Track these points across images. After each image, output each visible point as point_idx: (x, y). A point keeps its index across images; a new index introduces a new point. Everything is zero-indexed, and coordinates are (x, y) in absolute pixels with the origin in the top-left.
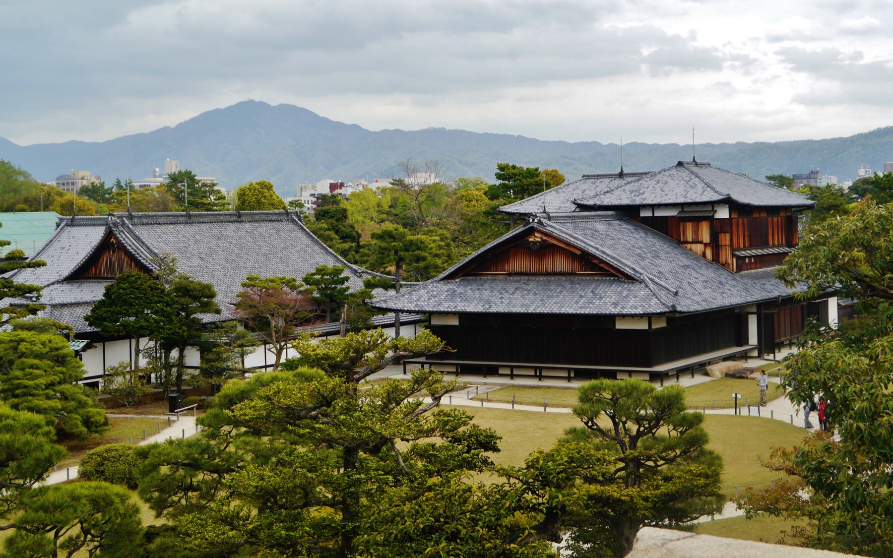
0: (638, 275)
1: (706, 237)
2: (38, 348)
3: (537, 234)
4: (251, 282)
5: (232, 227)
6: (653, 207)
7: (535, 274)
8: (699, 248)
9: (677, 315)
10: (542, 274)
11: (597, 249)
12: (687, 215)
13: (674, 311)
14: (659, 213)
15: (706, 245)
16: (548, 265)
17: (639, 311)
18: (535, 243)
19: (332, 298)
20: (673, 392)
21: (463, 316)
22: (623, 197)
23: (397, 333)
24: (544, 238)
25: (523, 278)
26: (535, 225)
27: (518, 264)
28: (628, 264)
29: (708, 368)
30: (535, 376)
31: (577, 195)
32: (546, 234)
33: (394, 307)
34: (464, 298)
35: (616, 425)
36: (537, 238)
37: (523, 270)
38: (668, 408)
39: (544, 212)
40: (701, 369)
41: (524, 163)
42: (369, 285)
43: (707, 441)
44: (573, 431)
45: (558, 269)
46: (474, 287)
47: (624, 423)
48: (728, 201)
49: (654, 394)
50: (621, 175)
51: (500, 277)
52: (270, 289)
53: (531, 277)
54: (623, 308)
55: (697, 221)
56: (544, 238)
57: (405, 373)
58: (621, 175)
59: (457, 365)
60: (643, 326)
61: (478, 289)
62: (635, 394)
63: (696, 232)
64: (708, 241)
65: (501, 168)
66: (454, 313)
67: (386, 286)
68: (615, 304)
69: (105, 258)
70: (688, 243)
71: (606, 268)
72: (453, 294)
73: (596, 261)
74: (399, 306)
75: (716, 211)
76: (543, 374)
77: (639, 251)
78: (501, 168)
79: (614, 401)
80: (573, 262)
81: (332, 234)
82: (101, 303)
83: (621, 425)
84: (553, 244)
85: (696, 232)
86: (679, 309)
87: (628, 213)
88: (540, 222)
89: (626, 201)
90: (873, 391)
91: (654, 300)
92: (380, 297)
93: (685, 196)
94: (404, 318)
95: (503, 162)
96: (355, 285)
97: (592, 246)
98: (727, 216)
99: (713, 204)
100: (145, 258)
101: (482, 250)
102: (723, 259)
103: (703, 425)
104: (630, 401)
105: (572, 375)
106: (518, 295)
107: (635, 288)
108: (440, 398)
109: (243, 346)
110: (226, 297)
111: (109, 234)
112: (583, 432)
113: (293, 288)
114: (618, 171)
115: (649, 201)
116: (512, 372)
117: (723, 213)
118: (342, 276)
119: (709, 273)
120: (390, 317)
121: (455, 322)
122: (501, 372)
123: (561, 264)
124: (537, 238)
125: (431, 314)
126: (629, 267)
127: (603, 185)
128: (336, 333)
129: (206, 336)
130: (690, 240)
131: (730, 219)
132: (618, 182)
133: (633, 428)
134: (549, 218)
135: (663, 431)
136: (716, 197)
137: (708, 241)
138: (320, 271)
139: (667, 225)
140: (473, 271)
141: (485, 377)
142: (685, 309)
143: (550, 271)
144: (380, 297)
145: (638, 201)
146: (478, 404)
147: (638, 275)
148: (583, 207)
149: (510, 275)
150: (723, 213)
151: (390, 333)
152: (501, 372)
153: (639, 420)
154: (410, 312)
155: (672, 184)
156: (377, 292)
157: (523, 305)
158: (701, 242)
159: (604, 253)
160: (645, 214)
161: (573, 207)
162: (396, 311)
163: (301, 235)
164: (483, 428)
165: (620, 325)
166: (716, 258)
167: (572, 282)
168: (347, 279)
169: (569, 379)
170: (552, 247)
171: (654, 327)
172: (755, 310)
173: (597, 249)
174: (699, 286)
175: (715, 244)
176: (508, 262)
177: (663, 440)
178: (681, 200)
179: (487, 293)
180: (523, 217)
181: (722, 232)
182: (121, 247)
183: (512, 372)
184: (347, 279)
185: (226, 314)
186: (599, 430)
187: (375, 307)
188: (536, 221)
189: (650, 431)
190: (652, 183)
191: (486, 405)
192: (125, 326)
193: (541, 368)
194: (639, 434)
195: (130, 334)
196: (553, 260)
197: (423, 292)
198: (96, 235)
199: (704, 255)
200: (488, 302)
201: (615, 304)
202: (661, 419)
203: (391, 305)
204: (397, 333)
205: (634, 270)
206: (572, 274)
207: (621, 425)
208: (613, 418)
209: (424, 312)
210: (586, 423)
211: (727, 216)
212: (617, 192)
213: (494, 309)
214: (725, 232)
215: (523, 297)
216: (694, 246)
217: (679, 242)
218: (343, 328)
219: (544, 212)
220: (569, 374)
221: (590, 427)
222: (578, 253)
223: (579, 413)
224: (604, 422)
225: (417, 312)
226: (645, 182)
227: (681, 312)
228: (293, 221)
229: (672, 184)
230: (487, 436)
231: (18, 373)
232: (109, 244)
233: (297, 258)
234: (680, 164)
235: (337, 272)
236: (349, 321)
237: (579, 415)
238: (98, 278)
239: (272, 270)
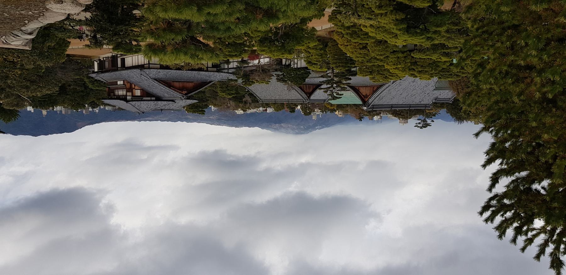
2: (315, 66)
4: (268, 82)
5: (277, 98)
6: (151, 100)
16: (181, 85)
17: (152, 70)
22: (160, 104)
27: (191, 85)
28: (156, 84)
31: (175, 105)
36: (184, 92)
48: (127, 101)
50: (162, 110)
52: (263, 80)
67: (231, 80)
68: (159, 72)
69: (311, 90)
82: (307, 77)
87: (158, 99)
89: (159, 102)
94: (226, 71)
96: (240, 81)
97: (167, 89)
99: (132, 101)
100: (299, 90)
101: (201, 89)
102: (129, 84)
107: (154, 77)
109: (269, 65)
110: (274, 79)
111: (309, 97)
113: (257, 81)
119: (132, 80)
120: (230, 71)
123: (177, 84)
124: (184, 92)
125: (217, 72)
127: (167, 107)
128: (244, 67)
129: (278, 67)
132: (163, 108)
136: (131, 102)
138: (251, 85)
139: (147, 95)
140: (204, 83)
145: (155, 102)
148: (173, 101)
155: (145, 107)
160: (154, 98)
163: (259, 96)
166: (131, 84)
170: (180, 89)
174: (135, 77)
178: (142, 102)
182: (306, 93)
185: (274, 73)
190: (152, 107)
192: (300, 72)
195: (298, 69)
198: (312, 97)
201: (159, 72)
212: (162, 105)
217: (143, 90)
224: (134, 43)
226: (153, 108)
229: (145, 107)
231: (320, 60)
232: (310, 94)
233: (258, 89)
236: (241, 70)
238: (310, 85)
239: (264, 85)
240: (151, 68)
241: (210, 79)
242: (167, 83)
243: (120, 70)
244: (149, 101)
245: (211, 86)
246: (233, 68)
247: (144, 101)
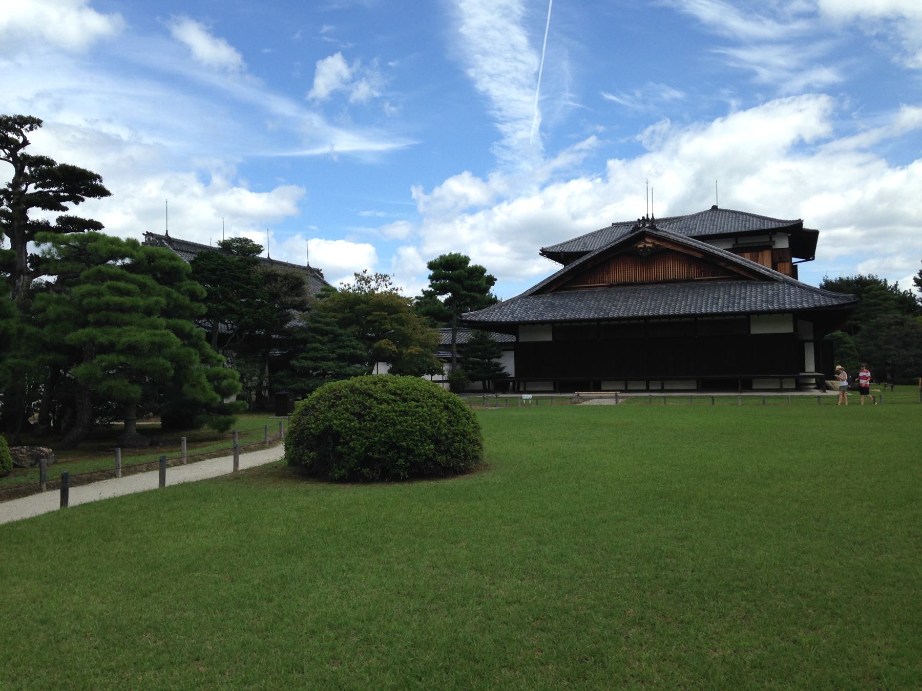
3: (647, 240)
7: (642, 284)
10: (650, 283)
24: (657, 243)
25: (627, 288)
27: (620, 273)
51: (599, 289)
56: (657, 243)
71: (734, 270)
73: (722, 264)
84: (668, 249)
121: (548, 338)
123: (674, 270)
124: (649, 243)
149: (611, 286)
165: (756, 330)
172: (811, 337)
176: (608, 273)
187: (466, 321)
188: (647, 225)
206: (689, 280)
214: (785, 262)
222: (699, 256)
228: (315, 277)
234: (715, 208)
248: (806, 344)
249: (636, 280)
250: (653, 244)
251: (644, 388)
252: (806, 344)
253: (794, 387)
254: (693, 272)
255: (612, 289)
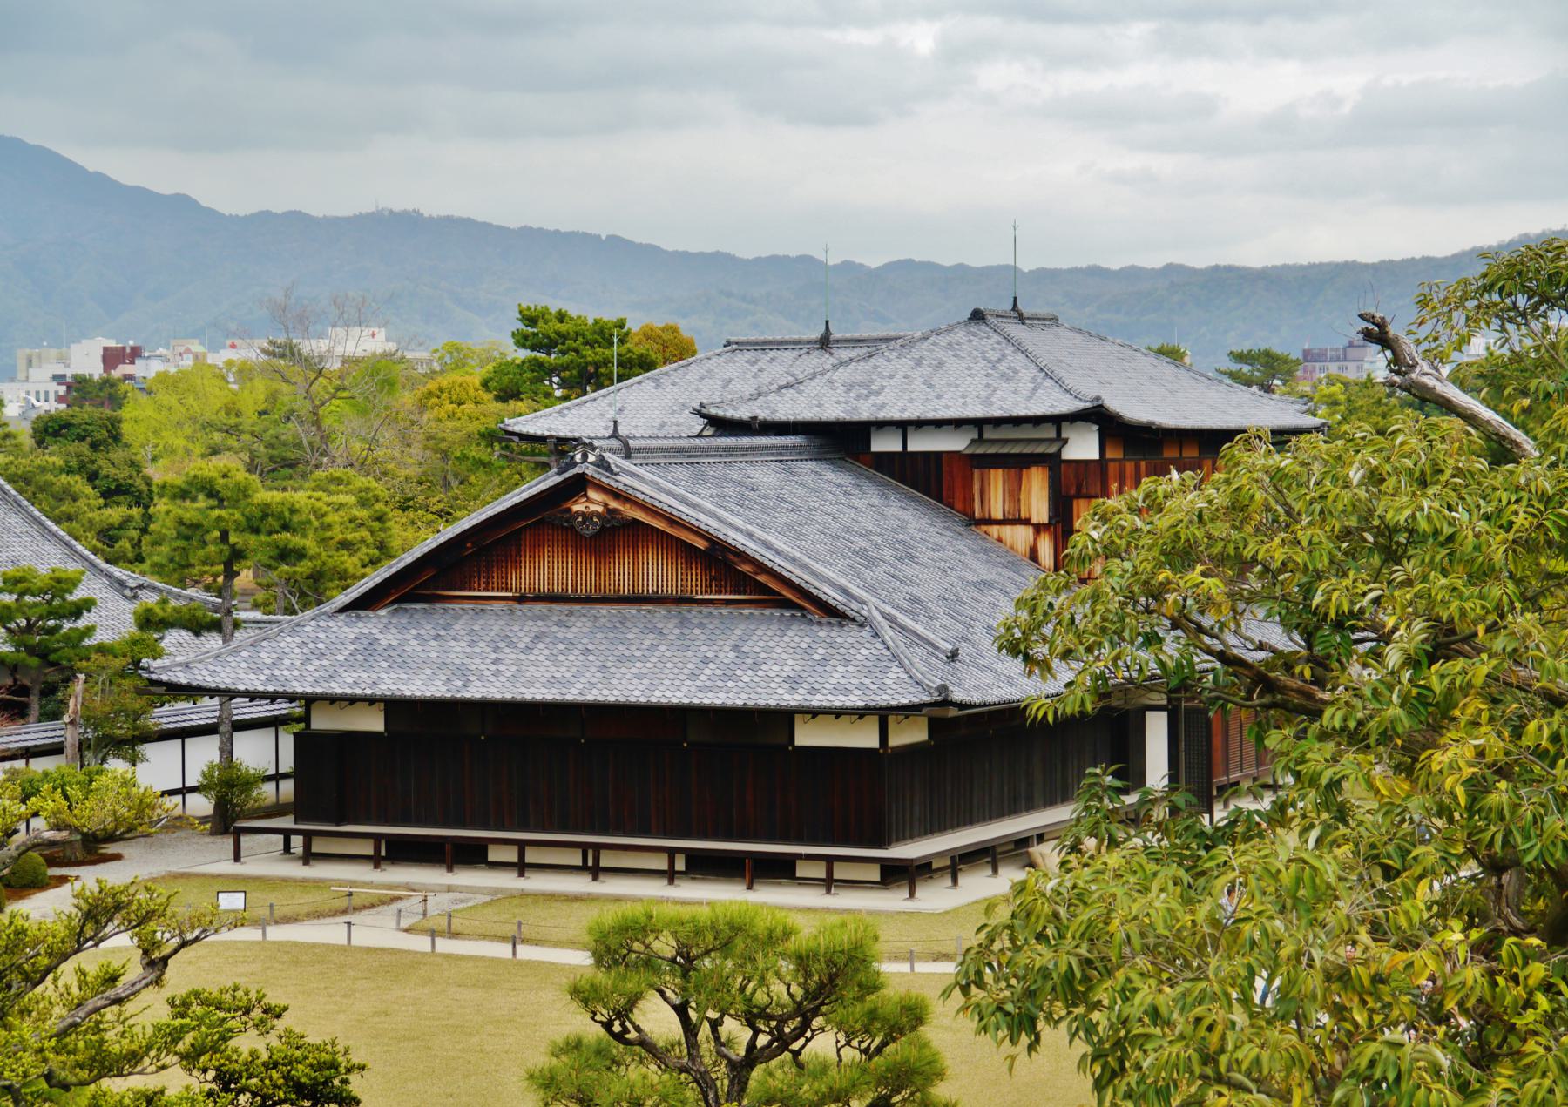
0: (855, 605)
1: (1038, 506)
3: (592, 494)
7: (588, 600)
8: (1020, 536)
9: (953, 712)
10: (605, 600)
11: (750, 535)
12: (992, 450)
13: (946, 703)
14: (920, 444)
15: (1038, 529)
16: (622, 573)
17: (855, 700)
18: (587, 517)
19: (43, 653)
20: (844, 939)
21: (395, 707)
23: (227, 751)
24: (613, 504)
25: (556, 607)
26: (590, 471)
27: (545, 570)
28: (828, 576)
29: (1036, 850)
30: (583, 868)
32: (616, 495)
33: (210, 681)
34: (398, 659)
35: (690, 1029)
36: (592, 503)
37: (557, 589)
38: (834, 979)
39: (615, 435)
40: (1018, 849)
41: (587, 306)
42: (148, 621)
43: (941, 1075)
44: (575, 1046)
45: (648, 587)
46: (427, 629)
47: (715, 1025)
49: (791, 946)
50: (825, 343)
51: (497, 606)
53: (576, 607)
54: (813, 691)
55: (1017, 464)
56: (613, 504)
57: (237, 858)
58: (825, 343)
59: (377, 837)
60: (865, 737)
61: (437, 637)
62: (740, 944)
63: (1014, 493)
64: (1046, 520)
65: (530, 319)
66: (371, 701)
67: (198, 627)
68: (793, 682)
70: (991, 521)
71: (773, 585)
72: (370, 648)
73: (746, 568)
74: (224, 680)
75: (1066, 441)
76: (603, 864)
77: (861, 543)
78: (530, 319)
79: (685, 962)
80: (688, 567)
81: (78, 483)
83: (705, 1030)
85: (1014, 492)
86: (958, 695)
87: (841, 442)
88: (602, 464)
89: (833, 411)
90: (1199, 1011)
91: (895, 672)
92: (179, 655)
93: (987, 402)
94: (243, 710)
95: (535, 300)
96: (110, 620)
98: (1095, 455)
99: (1057, 420)
101: (450, 532)
103: (927, 1032)
104: (729, 963)
105: (680, 865)
106: (541, 652)
107: (846, 637)
108: (164, 961)
112: (600, 1052)
114: (816, 334)
115: (895, 414)
116: (522, 855)
117: (1083, 446)
118: (78, 595)
121: (373, 722)
122: (494, 854)
123: (657, 572)
124: (592, 503)
125: (310, 700)
126: (833, 585)
127: (778, 367)
128: (56, 750)
130: (997, 514)
131: (1102, 462)
132: (817, 360)
133: (736, 1031)
134: (628, 453)
135: (823, 1045)
136: (1067, 405)
137: (1045, 519)
139: (938, 474)
140: (426, 584)
141: (450, 869)
142: (974, 697)
143: (626, 590)
144: (179, 655)
145: (865, 413)
146: (421, 943)
147: (855, 605)
148: (723, 426)
149: (521, 599)
150: (1083, 446)
151: (204, 753)
152: (492, 857)
153: (751, 1019)
154: (252, 696)
155: (953, 365)
156: (174, 639)
157: (553, 681)
158: (1027, 522)
159: (768, 546)
160: (884, 444)
161: (698, 424)
162: (230, 694)
164: (313, 1039)
165: (807, 736)
167: (683, 623)
168: (88, 605)
169: (671, 875)
171: (895, 741)
172: (1161, 699)
173: (750, 535)
175: (1061, 524)
176: (517, 565)
177: (824, 1068)
179: (458, 648)
180: (562, 447)
181: (1079, 496)
183: (522, 855)
184: (88, 605)
186: (644, 1043)
187: (159, 683)
189: (785, 1047)
190: (902, 365)
191: (444, 946)
193: (598, 848)
194: (754, 1056)
196: (636, 563)
197: (289, 642)
199: (1033, 555)
200: (463, 671)
201: (793, 682)
202: (816, 1012)
203: (202, 676)
204: (227, 751)
205: (845, 591)
206: (685, 601)
207: (706, 1029)
208: (681, 1010)
209: (291, 697)
210: (608, 1026)
211: (1094, 454)
212: (813, 387)
213: (475, 691)
215: (552, 658)
216: (1007, 532)
218: (70, 737)
219: (615, 435)
220: (672, 863)
221: (619, 1037)
222: (701, 544)
223: (585, 996)
224: (657, 1019)
225: (273, 697)
226: (890, 363)
227: (962, 706)
229: (953, 365)
230: (320, 1067)
234: (978, 316)
235: (61, 585)
236: (89, 720)
237: (585, 1002)
240: (861, 713)
241: (375, 624)
242: (730, 577)
243: (1148, 684)
244: (920, 424)
245: (345, 579)
246: (183, 734)
247: (958, 424)
248: (1150, 715)
249: (575, 590)
250: (606, 505)
251: (579, 862)
252: (1150, 715)
253: (877, 878)
254: (696, 577)
255: (525, 608)
